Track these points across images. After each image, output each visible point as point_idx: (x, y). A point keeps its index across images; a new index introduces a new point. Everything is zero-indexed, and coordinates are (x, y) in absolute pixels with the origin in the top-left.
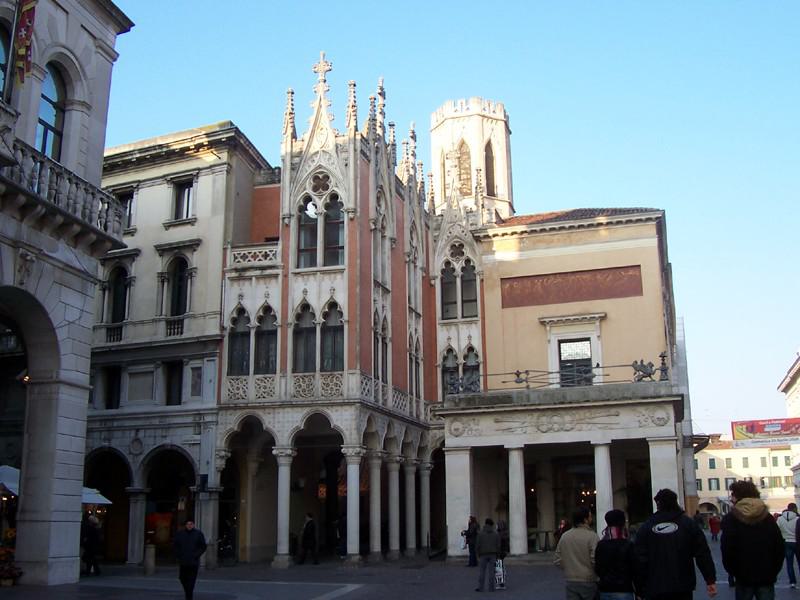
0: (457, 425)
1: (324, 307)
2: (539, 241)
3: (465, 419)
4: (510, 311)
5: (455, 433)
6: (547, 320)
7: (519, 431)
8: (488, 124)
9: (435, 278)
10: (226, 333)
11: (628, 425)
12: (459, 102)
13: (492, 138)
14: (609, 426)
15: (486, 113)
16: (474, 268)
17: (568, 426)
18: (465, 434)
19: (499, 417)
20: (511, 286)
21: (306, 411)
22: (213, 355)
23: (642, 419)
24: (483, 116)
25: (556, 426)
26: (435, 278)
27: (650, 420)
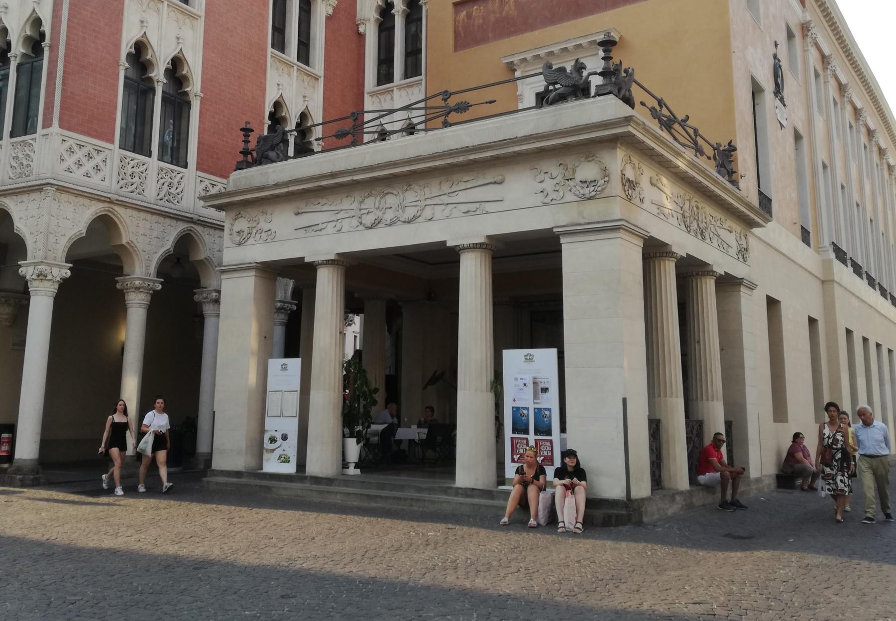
0: (242, 224)
3: (253, 212)
7: (330, 228)
9: (364, 21)
11: (519, 205)
14: (489, 207)
17: (410, 212)
18: (251, 241)
19: (302, 206)
20: (469, 16)
23: (549, 185)
25: (389, 216)
26: (364, 21)
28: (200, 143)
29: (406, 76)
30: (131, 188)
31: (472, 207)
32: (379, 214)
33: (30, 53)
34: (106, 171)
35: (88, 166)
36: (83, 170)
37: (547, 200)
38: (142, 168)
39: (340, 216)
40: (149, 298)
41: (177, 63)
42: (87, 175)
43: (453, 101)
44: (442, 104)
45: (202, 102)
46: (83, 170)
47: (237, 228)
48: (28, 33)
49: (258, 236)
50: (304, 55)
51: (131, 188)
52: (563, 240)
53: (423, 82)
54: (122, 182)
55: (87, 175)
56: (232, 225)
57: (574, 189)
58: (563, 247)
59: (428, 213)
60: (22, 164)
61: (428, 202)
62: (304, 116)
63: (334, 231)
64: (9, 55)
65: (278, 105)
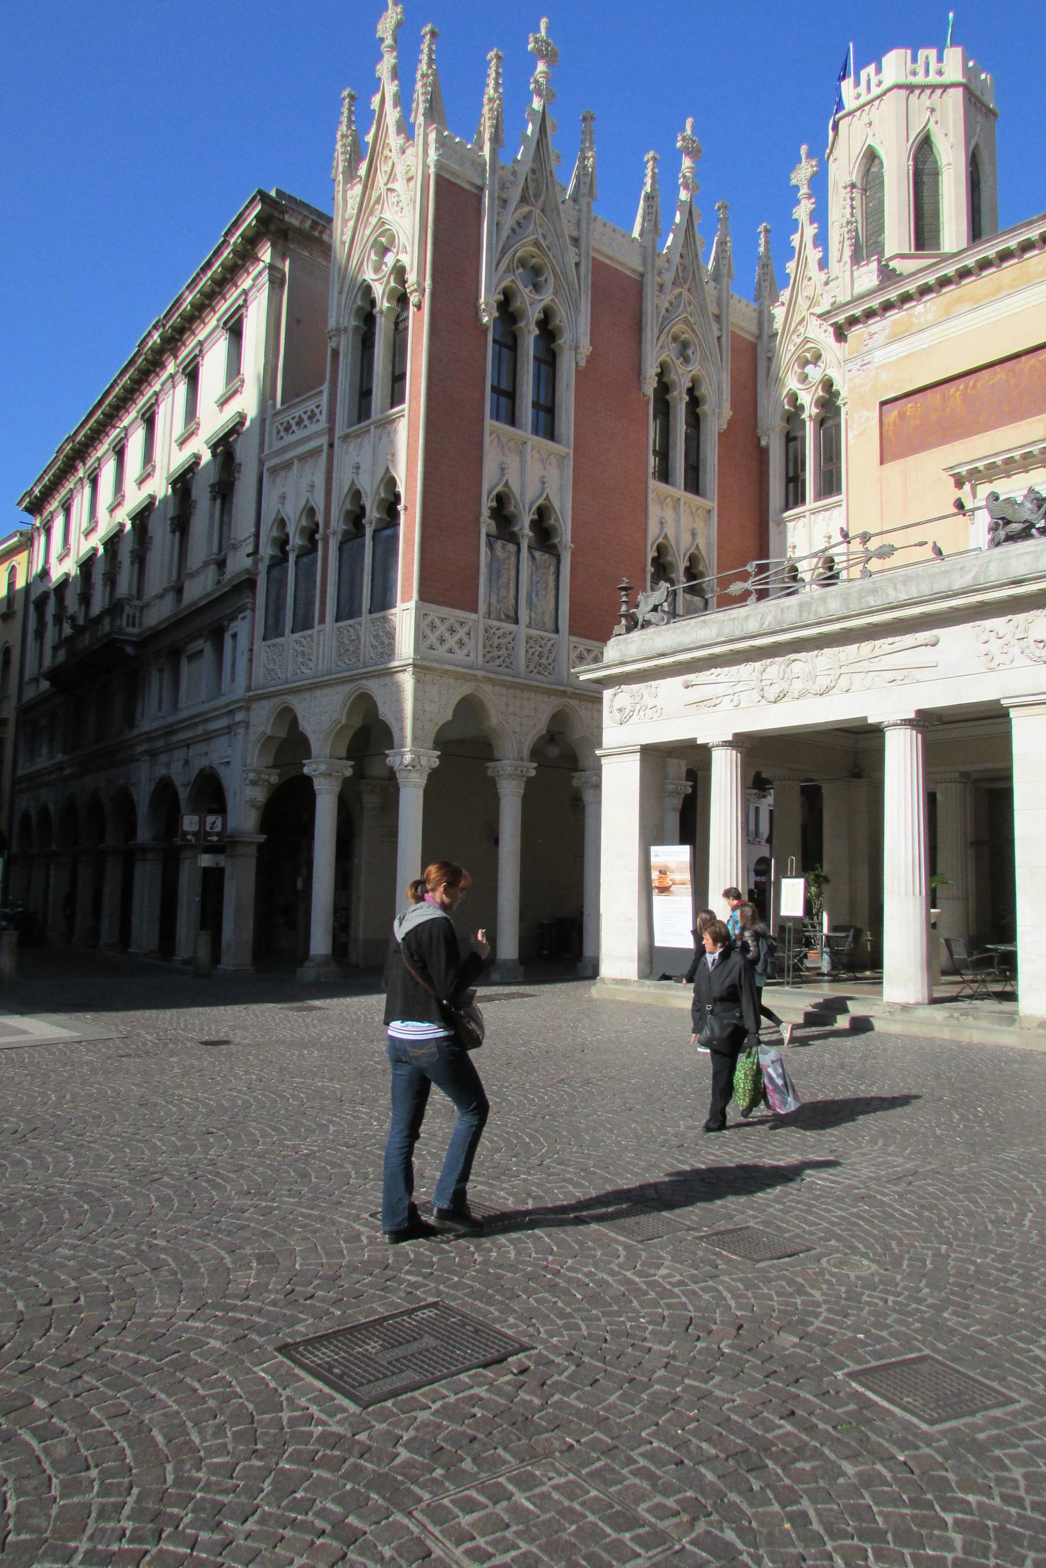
1: (377, 492)
2: (960, 300)
4: (894, 467)
5: (618, 716)
6: (963, 470)
7: (726, 702)
8: (921, 102)
10: (263, 567)
11: (957, 670)
12: (863, 74)
13: (931, 126)
14: (919, 674)
15: (920, 79)
16: (837, 394)
17: (823, 682)
20: (902, 416)
21: (347, 688)
22: (242, 609)
23: (995, 646)
24: (910, 88)
25: (798, 686)
27: (1015, 650)
28: (572, 603)
29: (818, 497)
30: (498, 662)
31: (899, 675)
32: (784, 685)
33: (385, 516)
34: (470, 645)
35: (452, 641)
36: (446, 647)
37: (993, 665)
38: (509, 638)
39: (738, 688)
40: (523, 786)
41: (543, 512)
42: (451, 651)
43: (873, 545)
44: (861, 548)
45: (573, 555)
46: (446, 647)
47: (617, 705)
48: (383, 495)
49: (642, 713)
50: (694, 485)
51: (498, 662)
52: (1013, 713)
53: (844, 503)
54: (489, 656)
55: (451, 651)
56: (612, 701)
57: (1026, 652)
58: (1014, 722)
59: (843, 683)
60: (382, 643)
61: (844, 670)
62: (693, 560)
63: (731, 706)
64: (364, 521)
65: (661, 549)
